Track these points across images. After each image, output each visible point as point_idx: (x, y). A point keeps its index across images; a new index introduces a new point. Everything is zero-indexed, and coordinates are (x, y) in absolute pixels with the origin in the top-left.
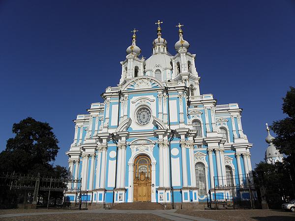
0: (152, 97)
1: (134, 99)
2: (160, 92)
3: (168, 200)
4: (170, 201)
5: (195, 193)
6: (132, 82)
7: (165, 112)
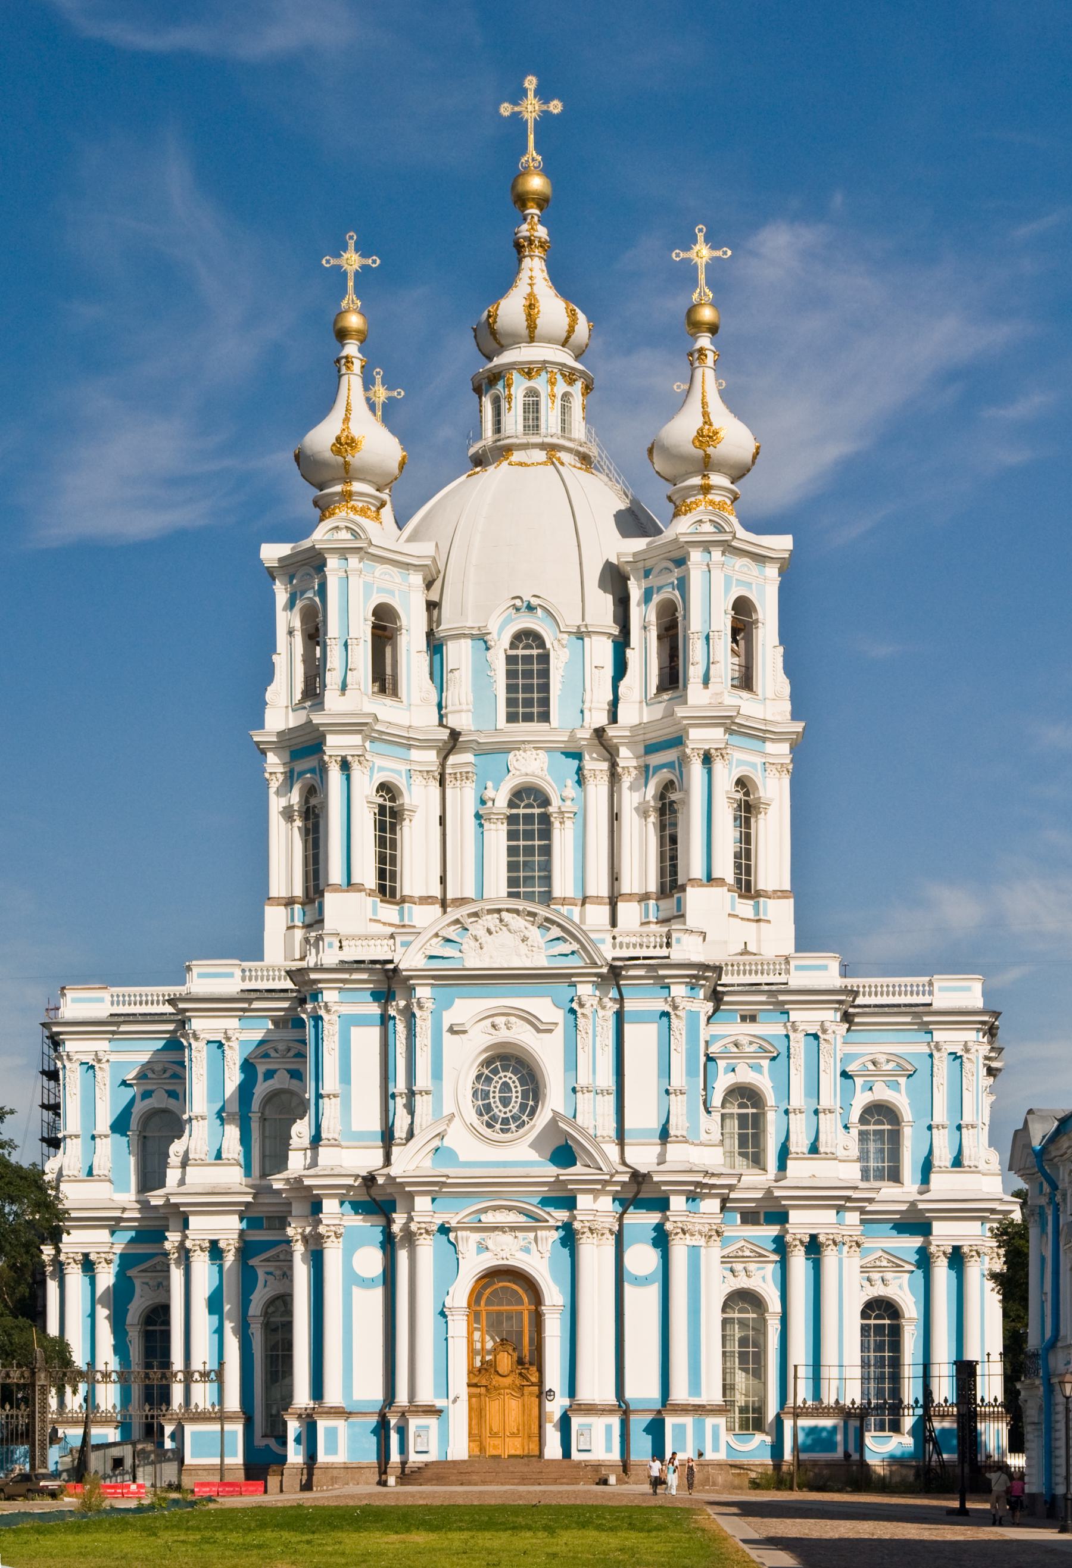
0: (544, 1008)
2: (585, 990)
3: (609, 1449)
4: (615, 1456)
5: (716, 1429)
6: (449, 925)
7: (606, 1079)
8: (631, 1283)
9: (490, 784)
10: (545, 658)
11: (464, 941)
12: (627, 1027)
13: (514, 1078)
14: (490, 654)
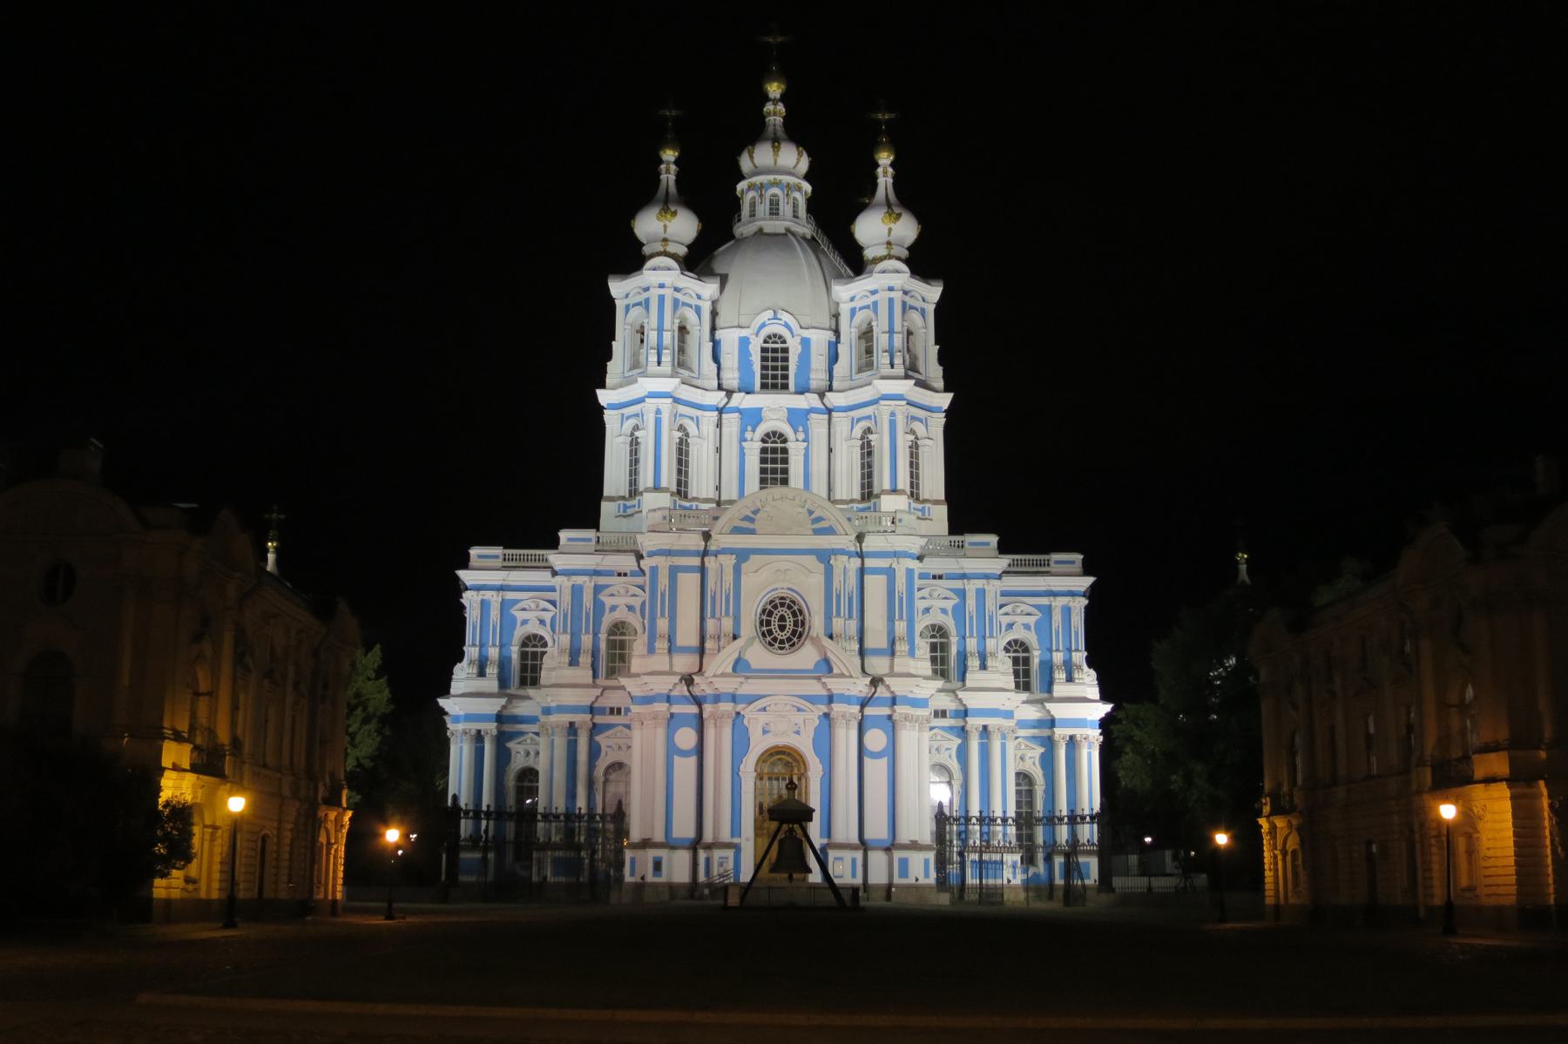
1: (755, 560)
8: (867, 756)
9: (749, 428)
10: (786, 350)
11: (758, 516)
12: (867, 578)
13: (789, 612)
14: (751, 347)
